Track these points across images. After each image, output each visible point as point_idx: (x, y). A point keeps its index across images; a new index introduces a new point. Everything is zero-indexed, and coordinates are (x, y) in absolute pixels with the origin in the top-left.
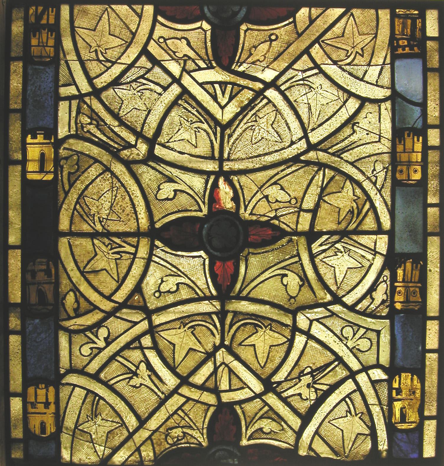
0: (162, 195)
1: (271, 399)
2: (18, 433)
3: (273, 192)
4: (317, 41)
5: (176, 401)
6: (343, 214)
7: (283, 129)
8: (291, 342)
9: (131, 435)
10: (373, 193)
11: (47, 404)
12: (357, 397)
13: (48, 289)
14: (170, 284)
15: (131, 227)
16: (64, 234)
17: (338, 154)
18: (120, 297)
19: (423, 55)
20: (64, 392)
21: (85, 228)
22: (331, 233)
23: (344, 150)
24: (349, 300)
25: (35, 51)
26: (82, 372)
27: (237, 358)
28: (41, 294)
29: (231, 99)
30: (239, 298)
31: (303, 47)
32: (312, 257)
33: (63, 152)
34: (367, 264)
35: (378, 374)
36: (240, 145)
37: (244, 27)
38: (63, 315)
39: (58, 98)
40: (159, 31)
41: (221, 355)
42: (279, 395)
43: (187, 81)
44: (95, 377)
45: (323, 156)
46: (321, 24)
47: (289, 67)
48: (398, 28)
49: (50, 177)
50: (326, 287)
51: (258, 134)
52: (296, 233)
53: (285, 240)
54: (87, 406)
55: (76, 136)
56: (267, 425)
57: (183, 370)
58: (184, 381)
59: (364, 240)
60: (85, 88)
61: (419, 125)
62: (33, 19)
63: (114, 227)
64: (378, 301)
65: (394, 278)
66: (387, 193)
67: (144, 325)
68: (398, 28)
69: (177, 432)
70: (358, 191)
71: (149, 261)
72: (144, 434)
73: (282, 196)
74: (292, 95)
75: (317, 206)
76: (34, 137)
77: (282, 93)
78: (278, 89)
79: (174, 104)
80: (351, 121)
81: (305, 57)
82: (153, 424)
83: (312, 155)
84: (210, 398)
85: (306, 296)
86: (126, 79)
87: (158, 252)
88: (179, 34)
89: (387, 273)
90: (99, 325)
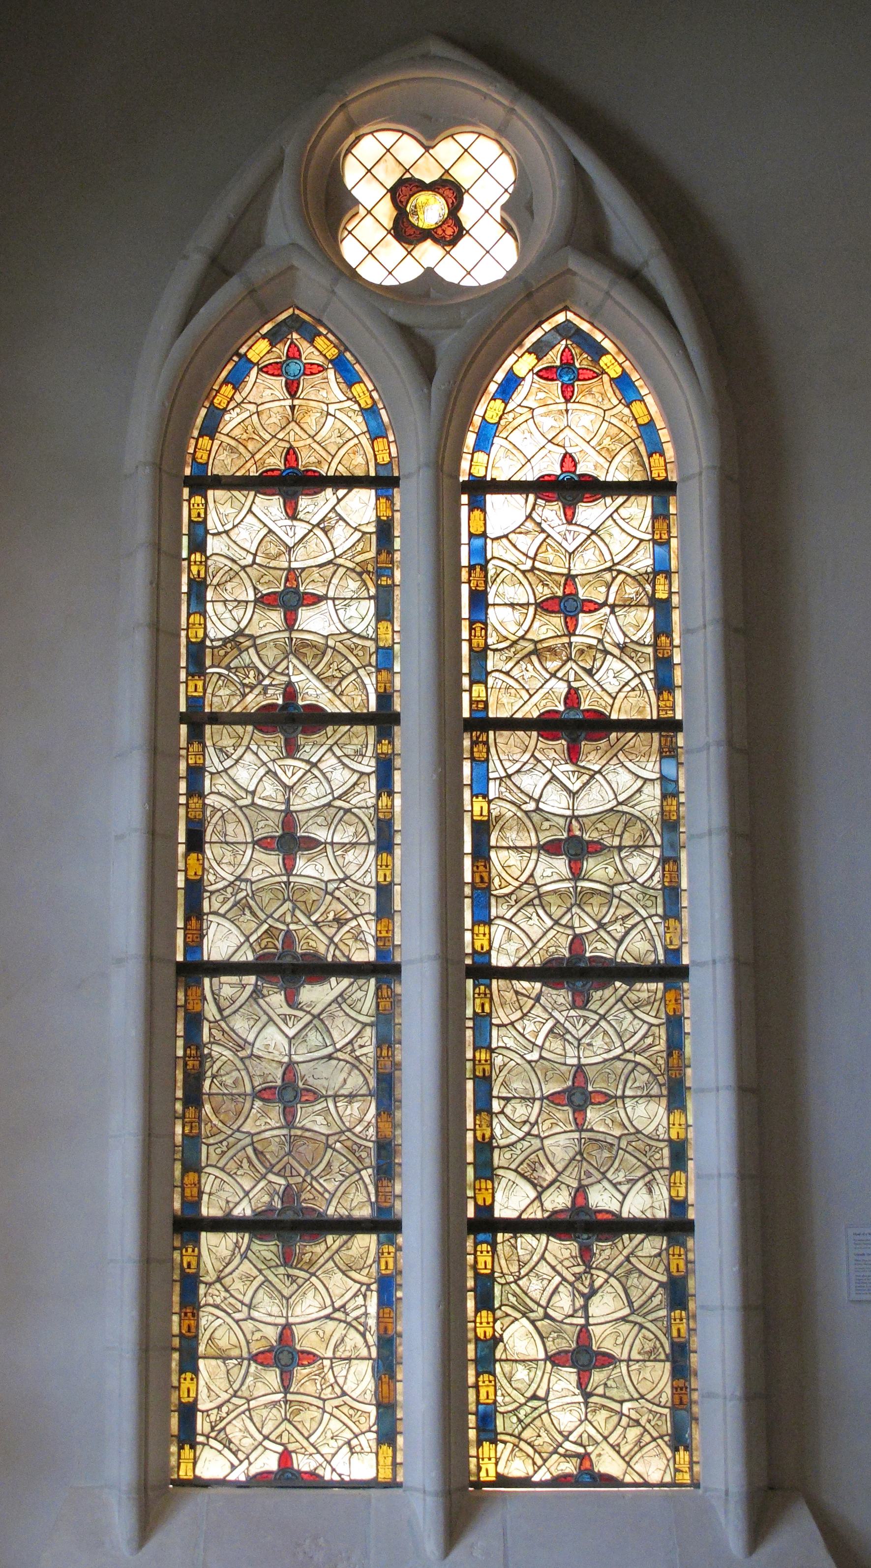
0: (543, 828)
1: (602, 933)
2: (468, 950)
3: (600, 826)
4: (621, 750)
5: (552, 933)
6: (636, 837)
7: (604, 794)
8: (611, 902)
9: (528, 951)
10: (651, 826)
11: (484, 934)
12: (646, 931)
13: (485, 875)
14: (548, 872)
15: (528, 844)
16: (493, 847)
17: (632, 807)
18: (523, 879)
19: (676, 756)
20: (493, 928)
21: (504, 844)
22: (630, 847)
23: (636, 805)
24: (640, 880)
25: (476, 755)
26: (503, 918)
27: (584, 910)
28: (482, 878)
29: (578, 779)
30: (583, 879)
31: (614, 752)
32: (621, 859)
33: (492, 806)
34: (649, 862)
35: (656, 919)
36: (582, 802)
37: (583, 743)
38: (493, 888)
39: (489, 779)
40: (540, 745)
41: (575, 910)
42: (605, 929)
43: (554, 770)
44: (510, 921)
45: (625, 808)
46: (623, 741)
47: (607, 763)
48: (663, 743)
49: (486, 818)
50: (629, 875)
51: (591, 797)
52: (612, 847)
53: (606, 851)
54: (506, 935)
55: (499, 798)
56: (600, 945)
57: (555, 917)
58: (556, 922)
59: (647, 850)
60: (503, 774)
61: (675, 792)
62: (474, 738)
63: (518, 844)
64: (655, 881)
65: (664, 870)
66: (659, 826)
67: (535, 894)
68: (663, 743)
69: (552, 949)
70: (644, 826)
71: (537, 860)
72: (536, 950)
73: (604, 828)
74: (608, 777)
75: (623, 833)
76: (477, 797)
77: (604, 776)
78: (601, 774)
79: (549, 782)
80: (639, 790)
81: (615, 758)
82: (540, 945)
83: (619, 808)
84: (570, 932)
85: (618, 879)
86: (523, 770)
87: (541, 856)
88: (551, 747)
89: (660, 867)
90: (512, 893)
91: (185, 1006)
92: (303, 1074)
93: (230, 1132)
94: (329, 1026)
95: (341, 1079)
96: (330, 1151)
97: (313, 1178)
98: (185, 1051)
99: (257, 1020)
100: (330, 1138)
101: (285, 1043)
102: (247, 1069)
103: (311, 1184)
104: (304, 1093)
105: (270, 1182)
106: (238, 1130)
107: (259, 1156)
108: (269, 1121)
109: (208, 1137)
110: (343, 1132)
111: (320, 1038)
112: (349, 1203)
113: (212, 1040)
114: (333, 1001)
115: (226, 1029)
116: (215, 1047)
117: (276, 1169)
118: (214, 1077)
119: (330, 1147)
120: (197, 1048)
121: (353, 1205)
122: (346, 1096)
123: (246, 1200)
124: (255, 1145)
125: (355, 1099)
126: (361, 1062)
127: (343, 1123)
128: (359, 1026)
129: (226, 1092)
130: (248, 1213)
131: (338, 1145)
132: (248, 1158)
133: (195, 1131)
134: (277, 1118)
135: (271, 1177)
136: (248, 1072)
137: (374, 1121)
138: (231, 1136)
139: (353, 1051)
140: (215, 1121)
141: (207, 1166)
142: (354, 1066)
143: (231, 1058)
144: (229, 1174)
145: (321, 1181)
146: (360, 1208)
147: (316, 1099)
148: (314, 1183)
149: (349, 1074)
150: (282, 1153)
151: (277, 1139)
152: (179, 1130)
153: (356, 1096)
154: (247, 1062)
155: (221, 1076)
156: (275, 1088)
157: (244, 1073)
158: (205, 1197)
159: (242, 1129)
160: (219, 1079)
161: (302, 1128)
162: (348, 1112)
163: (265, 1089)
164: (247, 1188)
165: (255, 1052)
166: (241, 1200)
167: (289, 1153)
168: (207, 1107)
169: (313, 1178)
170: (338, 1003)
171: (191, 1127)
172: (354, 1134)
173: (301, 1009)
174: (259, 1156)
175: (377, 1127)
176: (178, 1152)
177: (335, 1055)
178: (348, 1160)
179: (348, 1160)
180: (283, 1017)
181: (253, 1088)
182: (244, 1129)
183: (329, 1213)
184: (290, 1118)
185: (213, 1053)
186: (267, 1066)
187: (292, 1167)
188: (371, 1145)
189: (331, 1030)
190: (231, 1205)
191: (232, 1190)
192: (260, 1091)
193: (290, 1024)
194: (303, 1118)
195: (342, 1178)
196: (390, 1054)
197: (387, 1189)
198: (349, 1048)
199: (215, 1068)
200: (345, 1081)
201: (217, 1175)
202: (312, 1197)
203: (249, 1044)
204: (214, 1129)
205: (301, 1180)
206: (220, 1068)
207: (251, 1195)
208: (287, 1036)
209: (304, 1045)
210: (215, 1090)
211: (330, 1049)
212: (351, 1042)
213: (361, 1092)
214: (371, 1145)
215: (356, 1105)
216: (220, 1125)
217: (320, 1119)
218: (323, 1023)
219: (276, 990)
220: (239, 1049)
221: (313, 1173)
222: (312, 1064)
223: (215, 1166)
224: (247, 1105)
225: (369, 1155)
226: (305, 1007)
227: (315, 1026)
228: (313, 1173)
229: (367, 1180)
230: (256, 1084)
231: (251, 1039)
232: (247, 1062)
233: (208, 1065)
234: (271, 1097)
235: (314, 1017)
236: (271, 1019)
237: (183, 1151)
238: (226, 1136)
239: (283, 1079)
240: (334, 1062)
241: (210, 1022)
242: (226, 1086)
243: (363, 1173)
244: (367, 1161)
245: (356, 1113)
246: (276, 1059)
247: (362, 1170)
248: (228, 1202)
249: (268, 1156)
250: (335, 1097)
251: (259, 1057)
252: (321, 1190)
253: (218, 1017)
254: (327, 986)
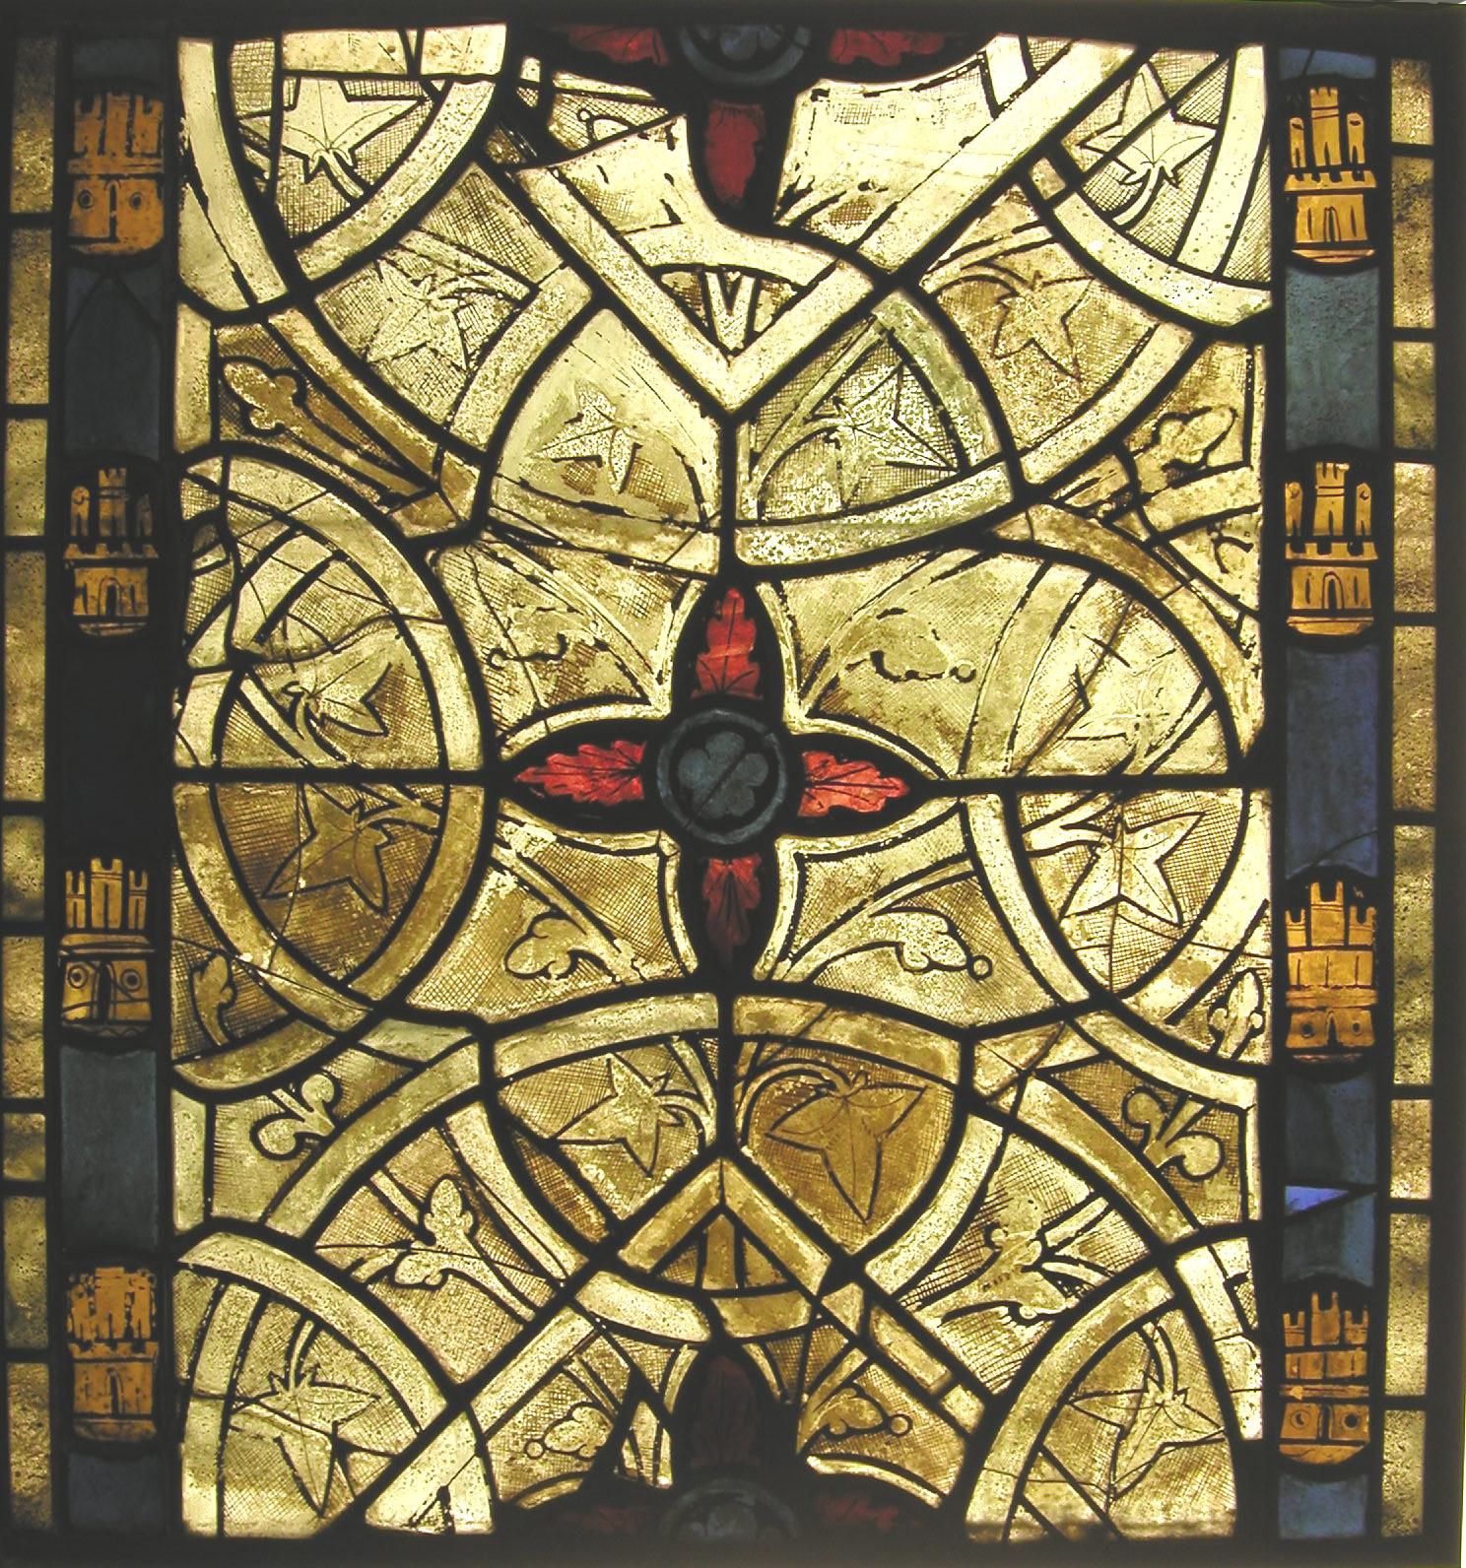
91: (57, 220)
96: (982, 1136)
97: (876, 1298)
98: (58, 502)
100: (986, 1051)
101: (701, 438)
102: (449, 615)
103: (864, 1340)
105: (605, 1328)
108: (596, 944)
110: (1061, 1016)
112: (1103, 1456)
114: (999, 187)
116: (249, 478)
118: (240, 663)
119: (985, 1107)
123: (457, 1437)
124: (513, 1098)
130: (473, 1513)
132: (466, 1177)
134: (646, 926)
135: (608, 1294)
137: (1259, 943)
138: (350, 1039)
139: (1134, 497)
140: (255, 948)
141: (211, 1225)
142: (1134, 591)
144: (343, 1278)
147: (897, 810)
148: (887, 1333)
149: (1109, 648)
150: (682, 1148)
152: (27, 999)
153: (1153, 782)
154: (455, 569)
155: (290, 658)
157: (433, 641)
158: (202, 1421)
159: (422, 997)
160: (277, 677)
161: (806, 990)
167: (725, 1147)
168: (204, 858)
170: (1033, 197)
175: (1281, 980)
176: (26, 1139)
178: (1100, 1187)
179: (1100, 1187)
180: (685, 280)
185: (235, 511)
187: (743, 1233)
190: (366, 1469)
191: (365, 1380)
192: (536, 753)
193: (731, 329)
194: (812, 924)
196: (1363, 517)
199: (251, 612)
200: (1081, 690)
202: (869, 1416)
205: (802, 1314)
206: (281, 611)
208: (709, 405)
210: (247, 744)
211: (990, 487)
212: (1114, 443)
213: (1179, 763)
214: (1242, 1091)
215: (1147, 846)
216: (284, 975)
217: (919, 933)
219: (637, 114)
221: (874, 1269)
222: (868, 581)
223: (258, 1231)
224: (461, 843)
225: (1231, 1159)
226: (822, 224)
230: (510, 710)
231: (475, 422)
232: (455, 569)
233: (204, 589)
235: (883, 281)
236: (603, 297)
237: (53, 1138)
238: (319, 1042)
240: (1010, 571)
241: (218, 317)
242: (321, 727)
243: (1195, 1267)
245: (1148, 889)
247: (1187, 1245)
248: (342, 1450)
249: (591, 1171)
250: (1012, 789)
253: (268, 286)
254: (962, 91)
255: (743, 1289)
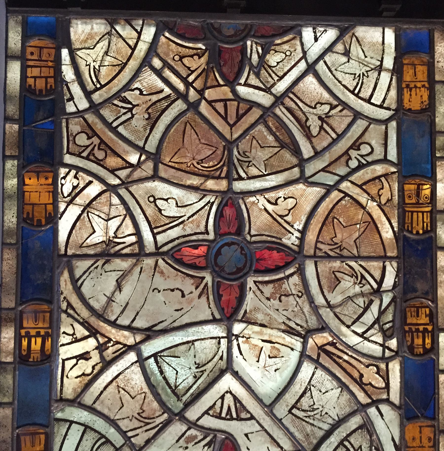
92: (204, 299)
93: (345, 185)
94: (150, 397)
95: (127, 289)
96: (151, 146)
97: (184, 97)
99: (293, 407)
100: (150, 172)
102: (315, 309)
103: (188, 85)
104: (202, 262)
105: (267, 90)
106: (329, 189)
107: (287, 141)
108: (270, 208)
109: (386, 175)
110: (126, 184)
111: (170, 373)
113: (383, 366)
115: (355, 389)
116: (377, 350)
117: (256, 113)
119: (149, 155)
120: (411, 349)
121: (104, 44)
122: (118, 255)
124: (295, 161)
125: (99, 250)
126: (85, 324)
127: (123, 202)
128: (88, 399)
129: (353, 264)
131: (133, 158)
132: (309, 136)
133: (410, 188)
134: (254, 213)
136: (311, 301)
137: (62, 206)
139: (101, 348)
140: (372, 206)
141: (386, 122)
143: (344, 329)
144: (346, 106)
145: (167, 90)
146: (90, 36)
147: (178, 249)
148: (181, 87)
149: (110, 300)
150: (243, 145)
151: (254, 171)
155: (362, 294)
156: (258, 272)
157: (320, 300)
158: (389, 63)
161: (204, 192)
162: (114, 224)
163: (278, 269)
164: (310, 79)
165: (297, 343)
166: (321, 57)
169: (184, 97)
171: (418, 194)
172: (102, 180)
173: (207, 431)
174: (287, 140)
177: (139, 338)
178: (114, 130)
179: (114, 130)
181: (301, 272)
182: (317, 191)
183: (153, 30)
184: (228, 212)
185: (380, 340)
186: (274, 315)
187: (225, 119)
188: (68, 159)
189: (146, 389)
190: (339, 47)
191: (339, 75)
192: (287, 265)
193: (229, 399)
194: (204, 213)
195: (127, 95)
196: (25, 343)
197: (36, 72)
198: (109, 352)
199: (375, 309)
200: (119, 287)
201: (366, 106)
203: (310, 357)
204: (374, 191)
206: (366, 309)
207: (303, 66)
208: (236, 374)
209: (202, 358)
213: (89, 263)
215: (98, 238)
216: (363, 199)
218: (162, 403)
220: (329, 348)
221: (185, 107)
222: (186, 320)
223: (373, 121)
224: (311, 237)
225: (72, 138)
227: (179, 398)
228: (185, 107)
229: (76, 89)
230: (295, 279)
232: (313, 322)
234: (266, 253)
238: (353, 178)
239: (242, 289)
240: (140, 323)
241: (387, 401)
242: (353, 274)
243: (83, 104)
244: (75, 128)
246: (257, 328)
248: (347, 53)
249: (271, 138)
251: (290, 331)
252: (168, 73)
253: (372, 411)
255: (225, 101)
